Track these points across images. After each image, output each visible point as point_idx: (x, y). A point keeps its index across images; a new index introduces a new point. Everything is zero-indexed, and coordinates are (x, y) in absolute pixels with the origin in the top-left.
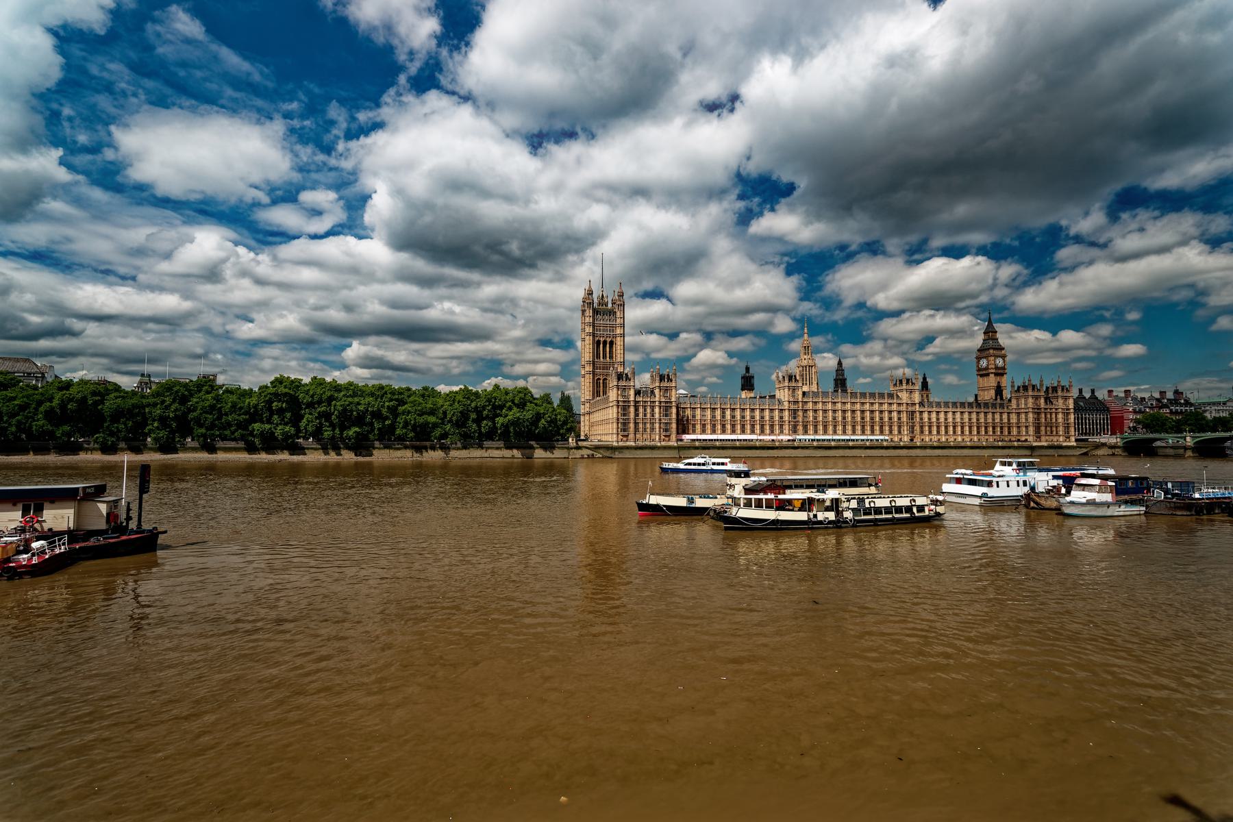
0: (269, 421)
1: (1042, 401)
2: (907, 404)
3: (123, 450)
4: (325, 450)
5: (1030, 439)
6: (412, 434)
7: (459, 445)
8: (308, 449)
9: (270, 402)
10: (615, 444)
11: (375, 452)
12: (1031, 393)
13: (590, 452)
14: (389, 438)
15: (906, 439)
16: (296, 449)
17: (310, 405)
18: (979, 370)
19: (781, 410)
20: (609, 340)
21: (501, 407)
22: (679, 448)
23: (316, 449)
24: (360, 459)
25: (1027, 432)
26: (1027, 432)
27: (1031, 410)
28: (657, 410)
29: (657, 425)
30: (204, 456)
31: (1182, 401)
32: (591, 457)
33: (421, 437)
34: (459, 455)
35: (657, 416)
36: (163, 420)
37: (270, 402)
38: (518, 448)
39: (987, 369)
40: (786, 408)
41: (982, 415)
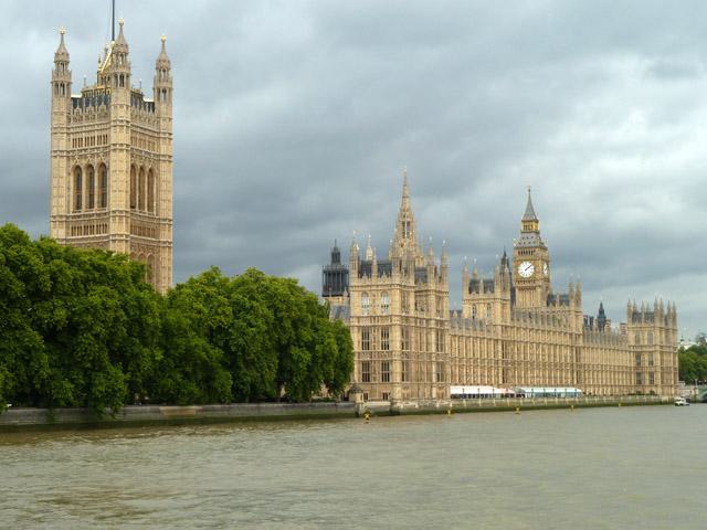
5: (659, 391)
12: (658, 324)
25: (652, 382)
26: (652, 382)
27: (658, 348)
39: (532, 279)
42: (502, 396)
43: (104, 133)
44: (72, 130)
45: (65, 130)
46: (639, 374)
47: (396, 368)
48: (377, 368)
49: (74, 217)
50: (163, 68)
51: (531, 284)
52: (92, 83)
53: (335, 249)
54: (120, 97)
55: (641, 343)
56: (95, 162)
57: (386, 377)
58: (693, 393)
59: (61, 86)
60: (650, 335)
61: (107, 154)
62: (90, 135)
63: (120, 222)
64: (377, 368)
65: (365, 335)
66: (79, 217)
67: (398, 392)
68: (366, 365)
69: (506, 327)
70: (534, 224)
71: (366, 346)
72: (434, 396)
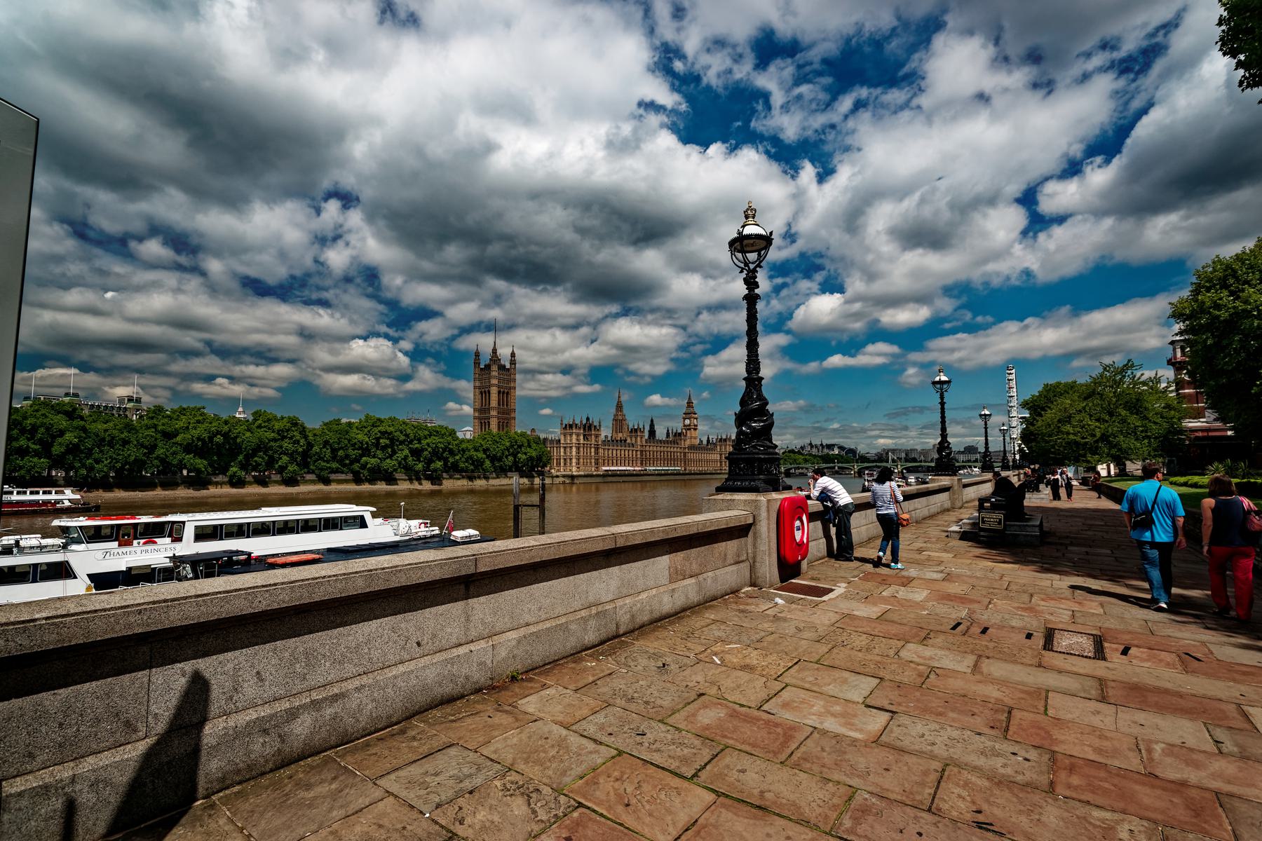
0: (374, 457)
3: (250, 483)
4: (411, 480)
6: (472, 467)
7: (494, 475)
8: (400, 479)
9: (378, 439)
11: (444, 482)
13: (563, 479)
14: (453, 470)
16: (391, 480)
17: (402, 443)
20: (506, 391)
21: (520, 447)
22: (603, 476)
23: (405, 480)
24: (436, 487)
30: (321, 487)
32: (564, 483)
33: (474, 470)
34: (495, 483)
36: (292, 455)
37: (378, 439)
38: (526, 477)
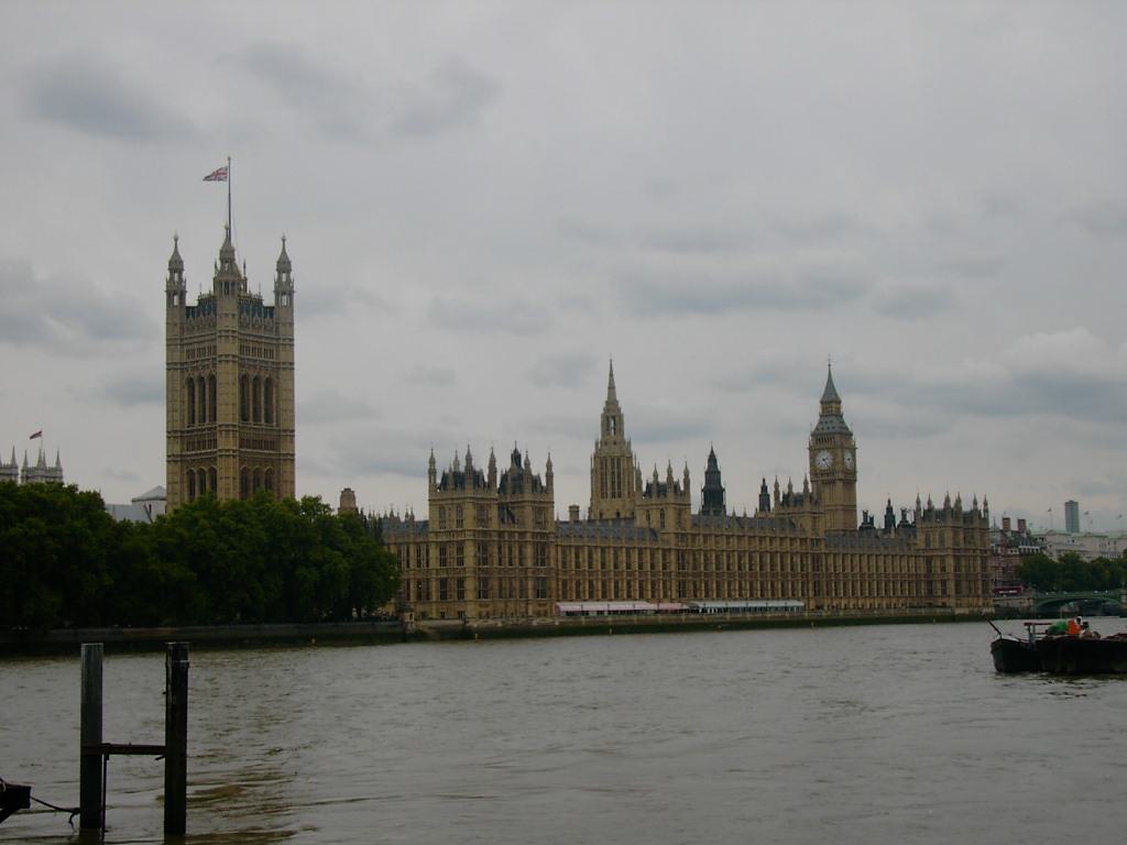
1: (961, 536)
2: (812, 540)
5: (951, 602)
10: (474, 624)
15: (812, 604)
18: (814, 472)
19: (666, 552)
20: (265, 375)
25: (944, 591)
26: (944, 591)
27: (950, 552)
28: (529, 551)
29: (530, 584)
31: (1025, 535)
35: (529, 563)
40: (673, 547)
41: (889, 560)
42: (657, 612)
43: (212, 344)
44: (185, 342)
45: (179, 342)
46: (930, 583)
47: (470, 585)
48: (453, 584)
49: (188, 432)
50: (284, 266)
51: (831, 477)
52: (208, 287)
53: (516, 451)
54: (228, 306)
55: (932, 547)
56: (206, 374)
57: (461, 595)
58: (1026, 604)
59: (175, 290)
60: (941, 536)
61: (215, 365)
62: (201, 346)
63: (227, 437)
64: (453, 584)
65: (443, 551)
66: (193, 431)
67: (471, 610)
68: (443, 583)
69: (683, 534)
70: (834, 405)
71: (443, 562)
72: (530, 613)
